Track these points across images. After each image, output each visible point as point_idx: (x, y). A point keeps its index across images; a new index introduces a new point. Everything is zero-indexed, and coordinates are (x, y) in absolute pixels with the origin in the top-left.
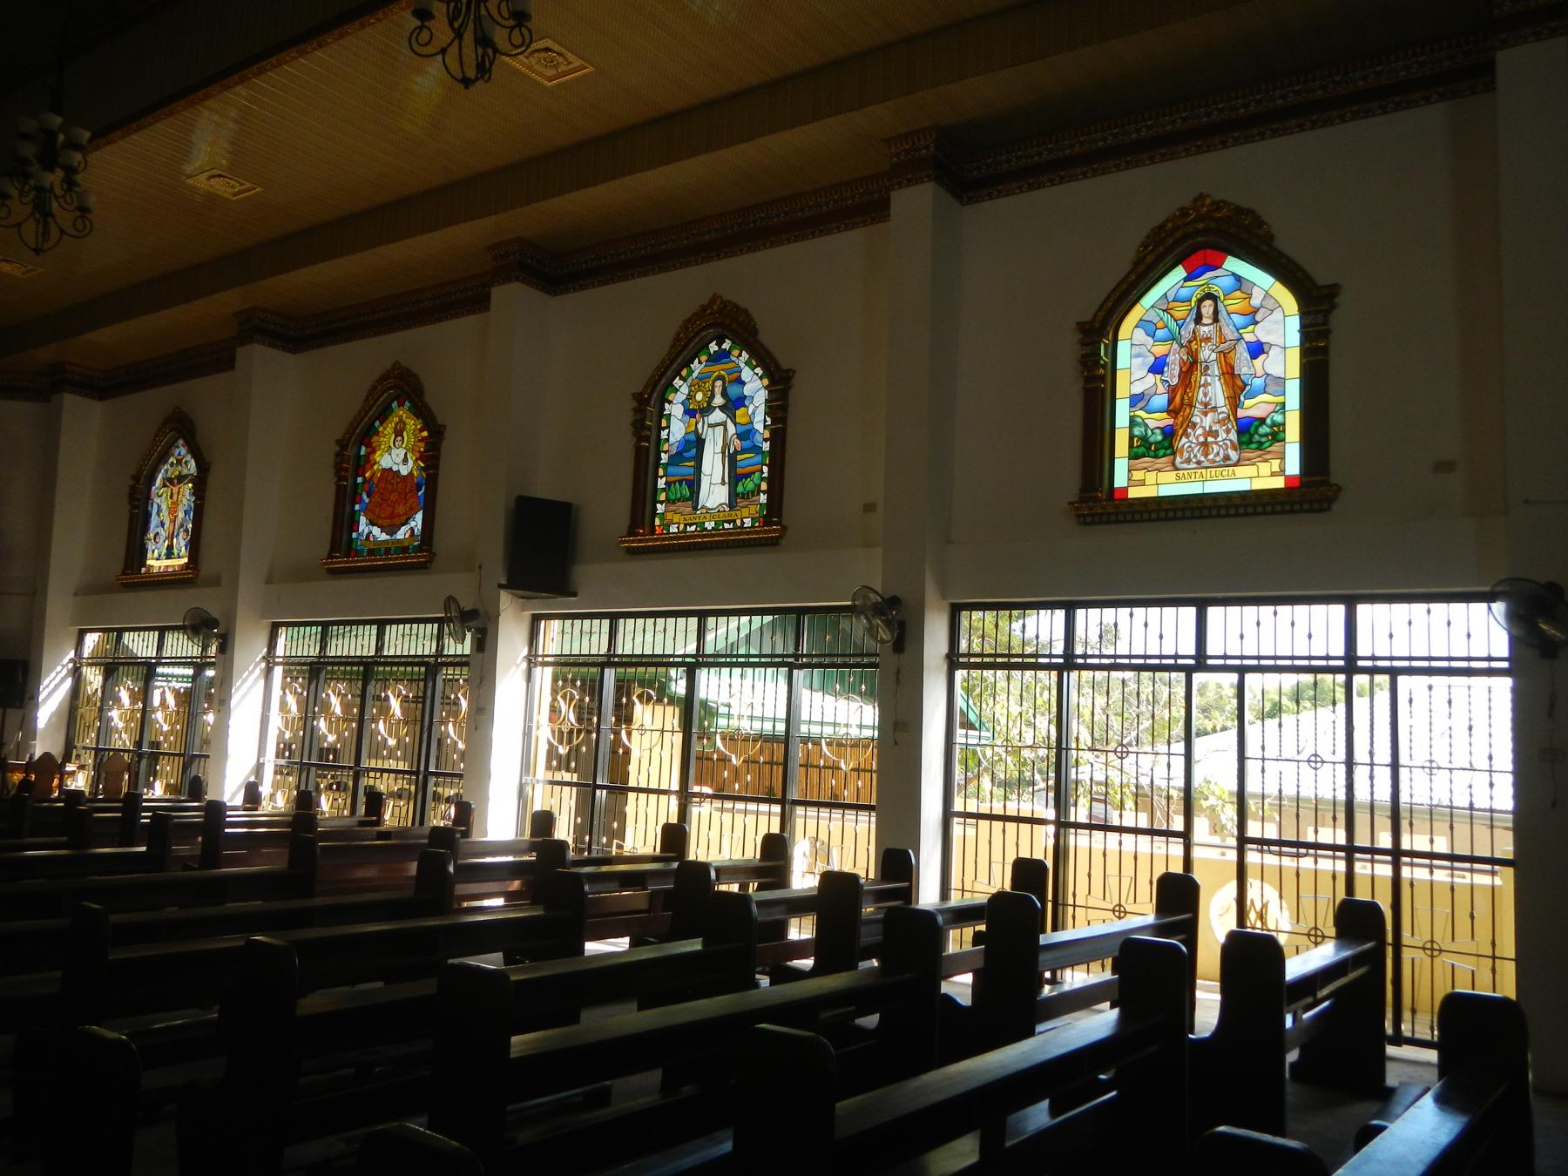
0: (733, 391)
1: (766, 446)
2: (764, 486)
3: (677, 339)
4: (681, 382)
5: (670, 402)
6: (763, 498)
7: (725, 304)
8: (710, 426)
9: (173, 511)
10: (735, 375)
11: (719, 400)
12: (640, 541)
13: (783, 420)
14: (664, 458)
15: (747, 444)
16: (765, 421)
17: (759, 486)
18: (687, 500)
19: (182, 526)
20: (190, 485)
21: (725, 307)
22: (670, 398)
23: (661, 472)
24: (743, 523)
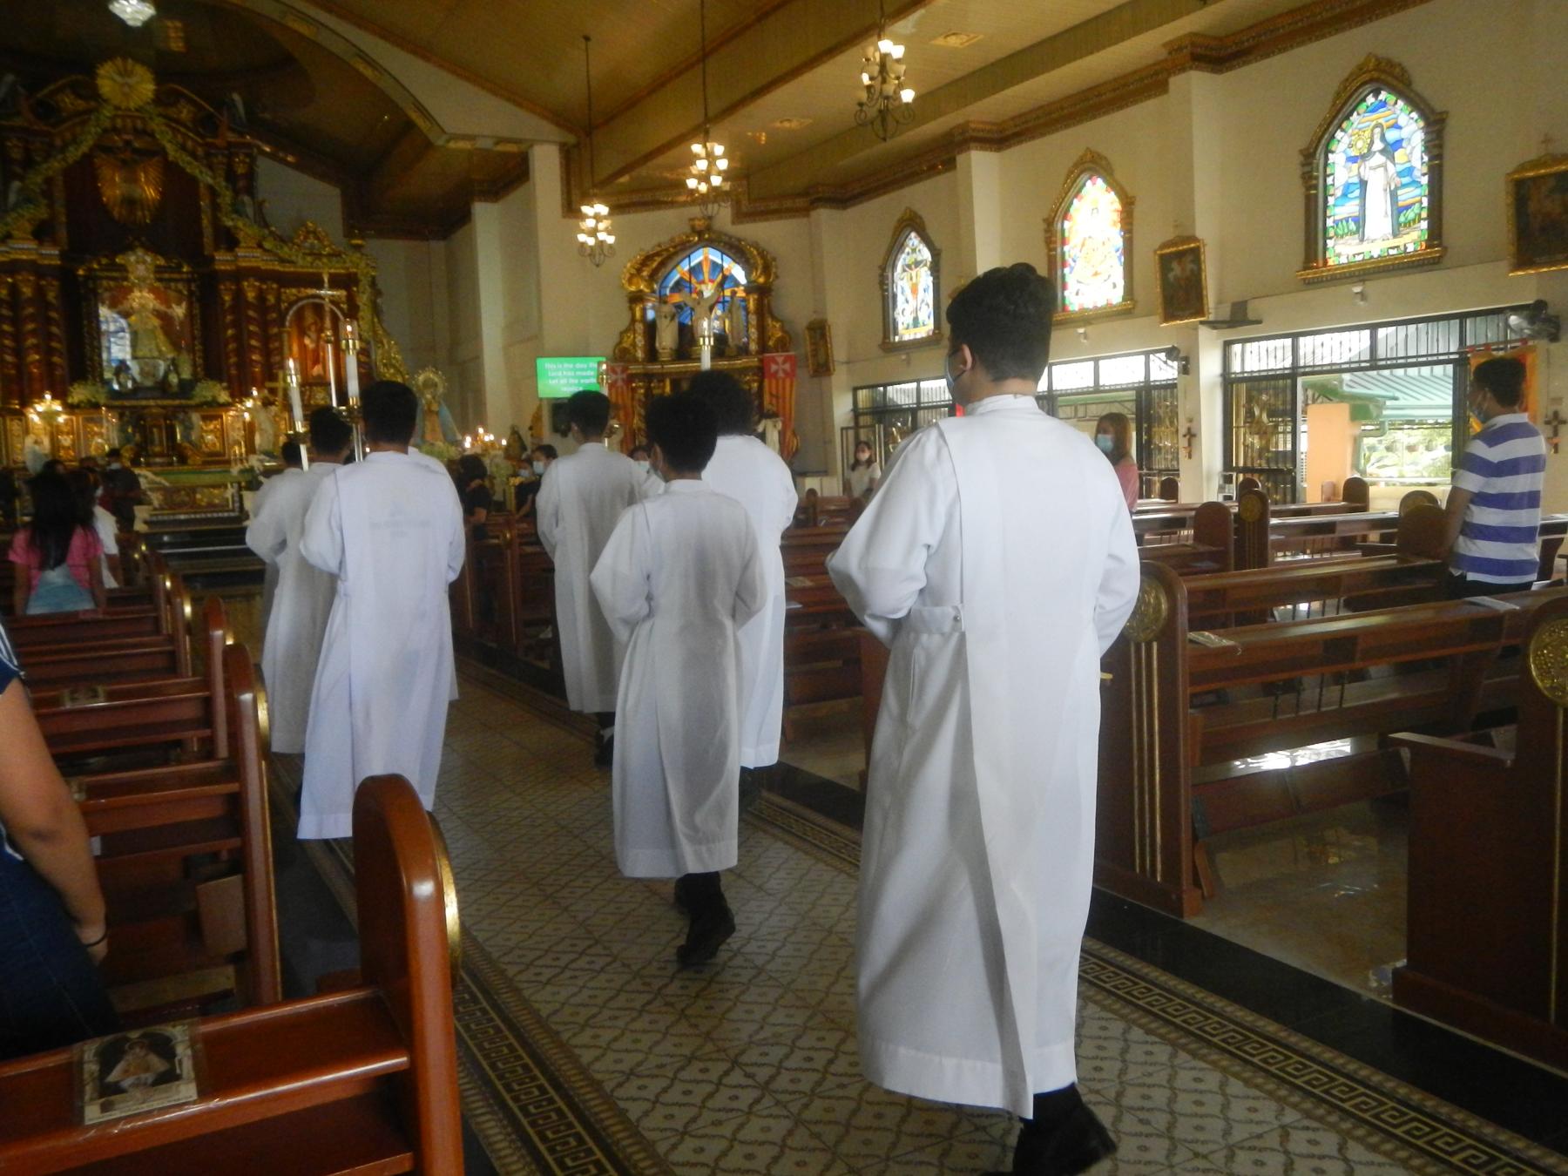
0: (1392, 136)
1: (1425, 180)
2: (1424, 214)
3: (1338, 95)
4: (1343, 134)
5: (1333, 152)
6: (1424, 225)
7: (1379, 61)
8: (1371, 168)
9: (914, 291)
10: (1391, 122)
11: (1378, 145)
12: (1315, 273)
13: (1439, 157)
14: (1331, 200)
15: (1406, 180)
16: (1422, 158)
17: (1420, 215)
18: (1355, 234)
19: (923, 301)
20: (926, 268)
21: (1380, 63)
22: (1333, 149)
23: (1328, 213)
24: (1406, 248)
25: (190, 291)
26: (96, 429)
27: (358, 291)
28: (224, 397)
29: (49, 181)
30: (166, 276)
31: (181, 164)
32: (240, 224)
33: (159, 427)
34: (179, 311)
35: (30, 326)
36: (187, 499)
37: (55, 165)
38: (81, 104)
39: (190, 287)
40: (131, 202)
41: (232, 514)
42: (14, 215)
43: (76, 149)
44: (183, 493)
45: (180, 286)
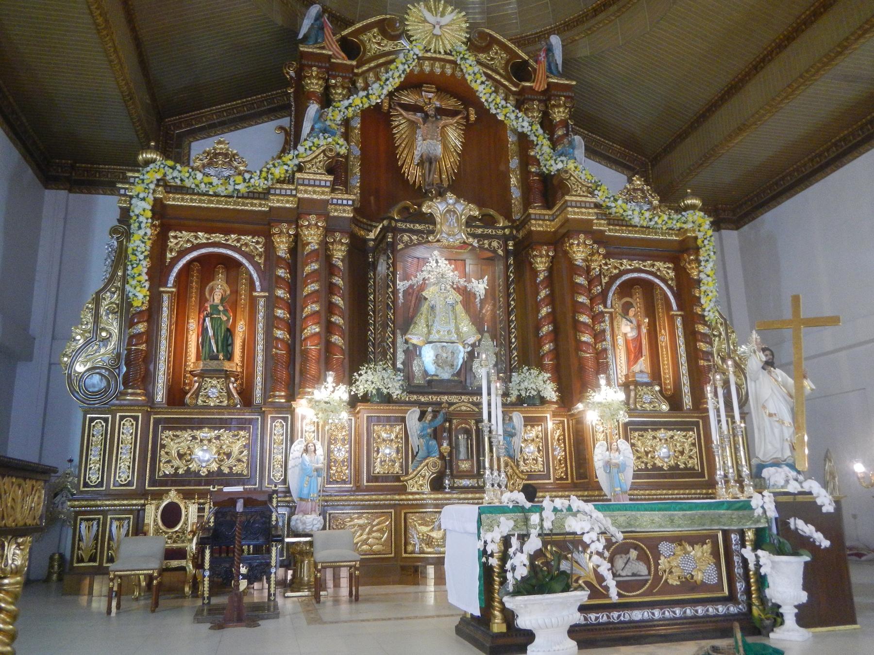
25: (507, 251)
26: (384, 435)
27: (698, 261)
28: (550, 392)
29: (346, 122)
30: (479, 231)
31: (493, 111)
32: (571, 165)
33: (468, 432)
34: (480, 287)
35: (313, 287)
36: (642, 569)
37: (358, 101)
38: (388, 46)
39: (507, 245)
40: (427, 161)
41: (733, 609)
42: (308, 144)
43: (383, 88)
44: (633, 554)
45: (495, 244)
